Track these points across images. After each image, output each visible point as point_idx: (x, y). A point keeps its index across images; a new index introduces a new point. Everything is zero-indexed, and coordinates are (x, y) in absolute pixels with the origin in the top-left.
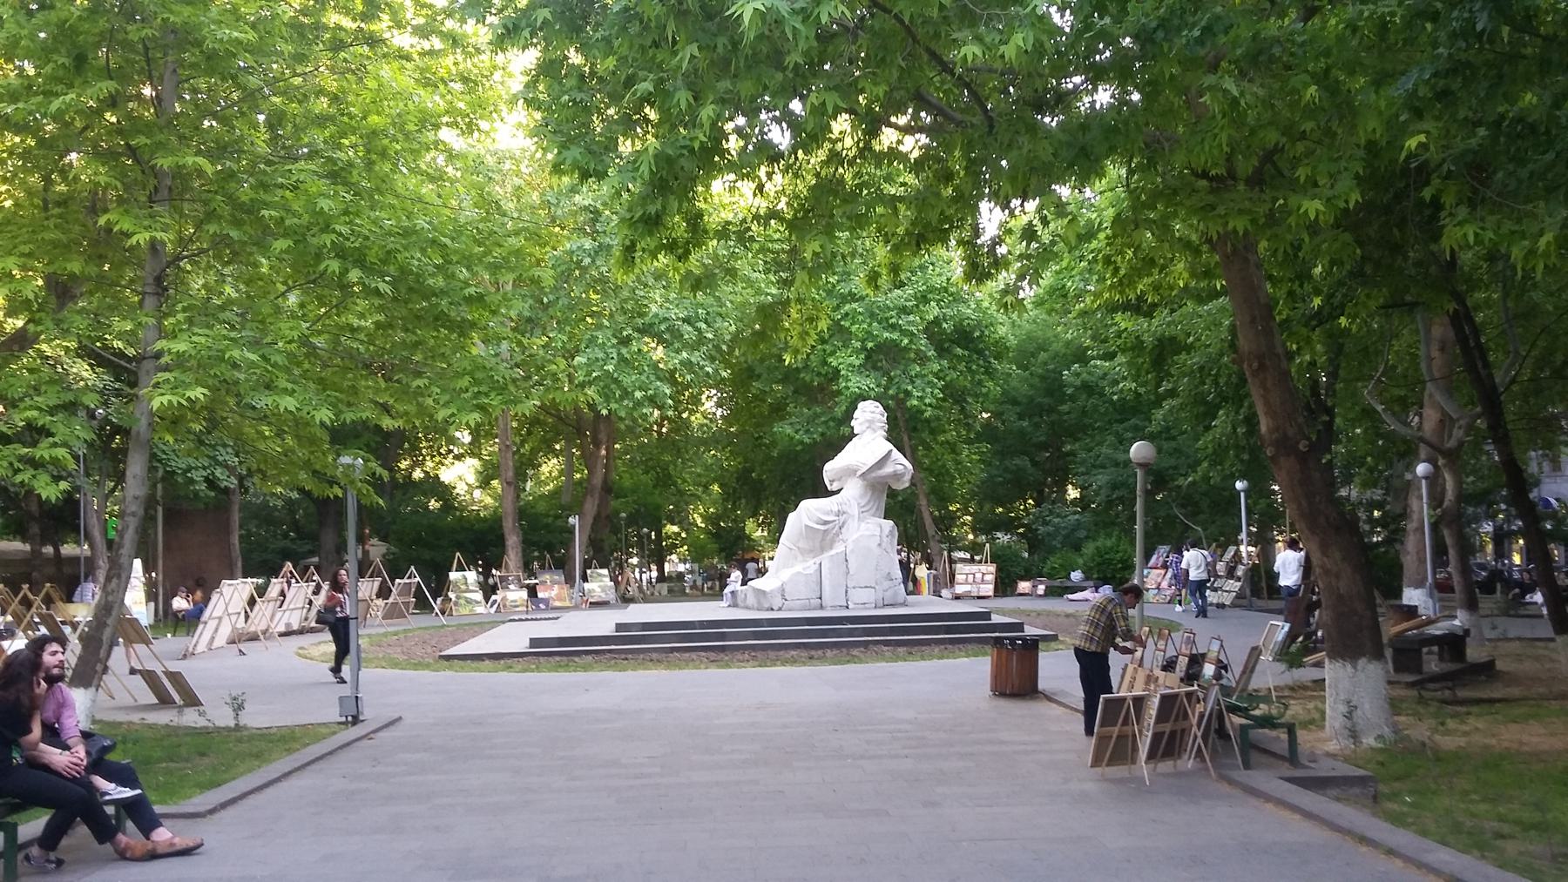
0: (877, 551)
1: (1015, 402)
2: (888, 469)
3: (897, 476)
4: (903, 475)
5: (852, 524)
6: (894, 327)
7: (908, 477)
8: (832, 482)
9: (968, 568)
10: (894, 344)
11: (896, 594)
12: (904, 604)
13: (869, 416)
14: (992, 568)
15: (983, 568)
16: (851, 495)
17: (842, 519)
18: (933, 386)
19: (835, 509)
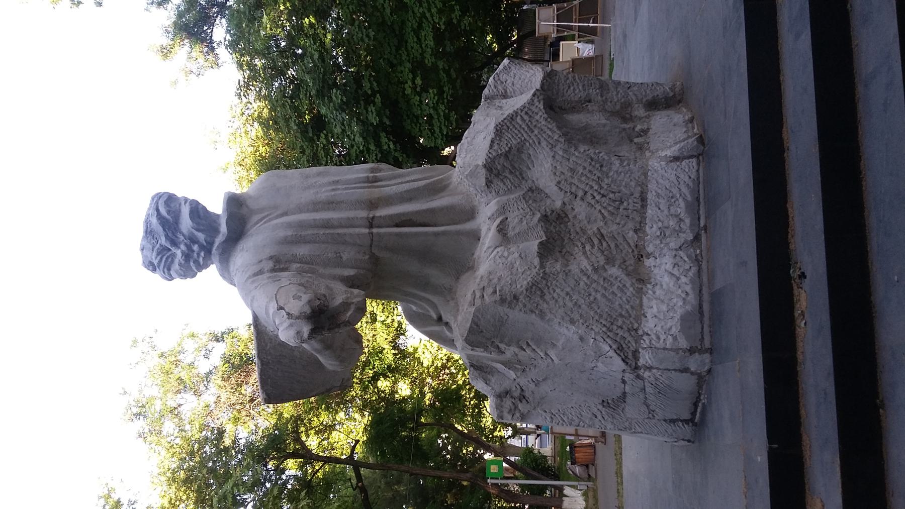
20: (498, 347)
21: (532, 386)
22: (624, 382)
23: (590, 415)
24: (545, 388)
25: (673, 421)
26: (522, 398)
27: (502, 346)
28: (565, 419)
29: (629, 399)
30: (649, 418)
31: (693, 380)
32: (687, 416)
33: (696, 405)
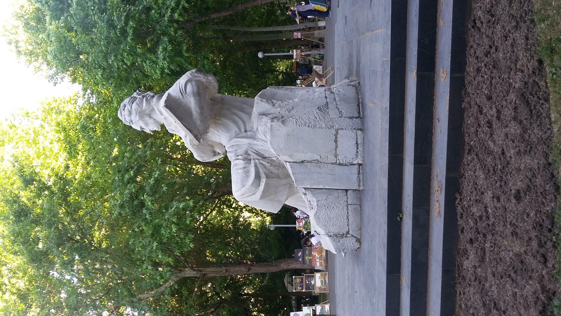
2: (192, 102)
3: (200, 93)
5: (259, 146)
7: (201, 77)
8: (215, 154)
10: (135, 30)
11: (344, 100)
12: (355, 75)
13: (135, 118)
16: (224, 140)
17: (253, 156)
19: (241, 163)
21: (287, 113)
22: (326, 97)
23: (313, 118)
24: (293, 112)
25: (351, 118)
26: (283, 117)
27: (274, 101)
28: (302, 122)
29: (330, 106)
30: (340, 117)
31: (354, 90)
32: (356, 115)
33: (358, 106)
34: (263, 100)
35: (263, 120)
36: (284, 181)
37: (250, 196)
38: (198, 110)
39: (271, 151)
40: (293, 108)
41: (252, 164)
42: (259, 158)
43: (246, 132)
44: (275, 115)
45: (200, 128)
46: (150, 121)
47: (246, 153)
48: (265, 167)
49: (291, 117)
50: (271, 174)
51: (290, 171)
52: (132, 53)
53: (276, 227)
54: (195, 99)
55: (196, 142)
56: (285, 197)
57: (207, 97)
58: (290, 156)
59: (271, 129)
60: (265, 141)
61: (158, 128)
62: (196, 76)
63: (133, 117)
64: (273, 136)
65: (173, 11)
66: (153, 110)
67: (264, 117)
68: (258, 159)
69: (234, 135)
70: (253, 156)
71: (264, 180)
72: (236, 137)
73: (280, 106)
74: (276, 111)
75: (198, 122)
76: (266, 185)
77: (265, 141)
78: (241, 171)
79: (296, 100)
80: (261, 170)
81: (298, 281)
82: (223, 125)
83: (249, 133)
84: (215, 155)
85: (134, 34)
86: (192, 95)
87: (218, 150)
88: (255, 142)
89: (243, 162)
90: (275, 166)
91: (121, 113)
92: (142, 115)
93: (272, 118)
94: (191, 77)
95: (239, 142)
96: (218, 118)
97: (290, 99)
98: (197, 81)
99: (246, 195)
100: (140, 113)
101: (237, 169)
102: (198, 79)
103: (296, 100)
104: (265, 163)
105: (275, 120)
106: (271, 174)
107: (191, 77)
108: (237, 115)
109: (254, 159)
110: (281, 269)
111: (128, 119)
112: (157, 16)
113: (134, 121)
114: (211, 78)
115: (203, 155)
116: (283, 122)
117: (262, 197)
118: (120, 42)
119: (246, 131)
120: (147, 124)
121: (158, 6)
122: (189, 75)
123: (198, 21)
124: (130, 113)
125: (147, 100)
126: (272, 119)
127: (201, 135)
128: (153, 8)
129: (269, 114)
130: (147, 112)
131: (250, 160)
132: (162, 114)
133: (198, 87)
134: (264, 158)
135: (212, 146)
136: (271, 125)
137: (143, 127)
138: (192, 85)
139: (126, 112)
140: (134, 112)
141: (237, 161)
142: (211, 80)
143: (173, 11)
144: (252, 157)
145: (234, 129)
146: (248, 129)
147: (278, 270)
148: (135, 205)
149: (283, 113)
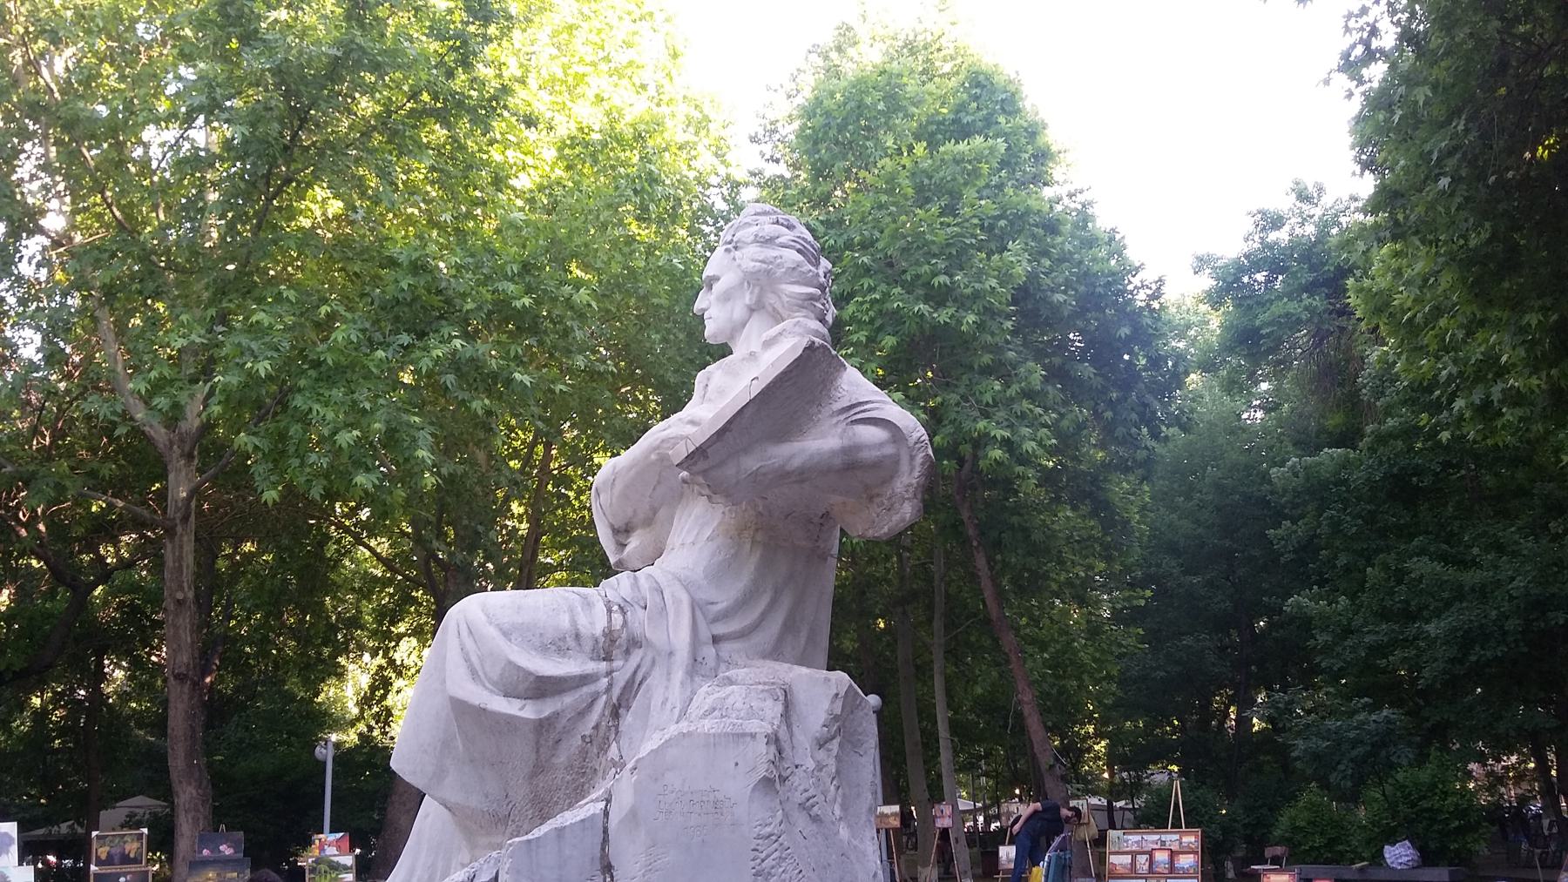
0: (754, 816)
1: (1172, 549)
2: (822, 441)
3: (857, 473)
4: (884, 469)
6: (939, 297)
7: (909, 477)
8: (622, 532)
9: (1133, 839)
13: (750, 257)
14: (1191, 839)
15: (1171, 838)
16: (683, 560)
17: (623, 669)
18: (1035, 423)
20: (833, 738)
21: (798, 798)
24: (801, 821)
26: (783, 780)
34: (839, 703)
35: (769, 702)
36: (520, 793)
37: (467, 660)
38: (796, 463)
39: (651, 733)
40: (816, 819)
41: (591, 667)
42: (616, 692)
43: (713, 645)
44: (787, 752)
45: (730, 471)
46: (739, 311)
47: (634, 643)
48: (582, 714)
49: (786, 815)
50: (550, 742)
51: (569, 818)
52: (878, 323)
53: (325, 763)
54: (833, 453)
55: (681, 452)
56: (455, 797)
57: (836, 499)
58: (633, 816)
59: (740, 736)
60: (684, 713)
61: (715, 336)
62: (912, 458)
63: (753, 251)
64: (714, 742)
65: (1007, 444)
66: (777, 318)
67: (779, 708)
68: (610, 685)
69: (702, 596)
70: (623, 669)
71: (526, 711)
72: (694, 605)
73: (820, 767)
74: (805, 755)
75: (751, 463)
76: (510, 720)
77: (684, 713)
78: (565, 622)
79: (844, 832)
80: (568, 699)
81: (128, 847)
82: (735, 556)
83: (709, 651)
84: (616, 531)
85: (936, 327)
86: (846, 442)
87: (634, 542)
88: (679, 675)
89: (598, 631)
90: (584, 754)
91: (765, 213)
92: (761, 280)
93: (777, 740)
94: (911, 442)
95: (678, 613)
96: (759, 537)
97: (844, 808)
98: (895, 459)
99: (469, 644)
100: (768, 272)
101: (571, 610)
102: (904, 466)
103: (844, 832)
104: (594, 716)
105: (773, 749)
106: (550, 742)
107: (911, 442)
108: (773, 603)
109: (609, 673)
110: (176, 787)
111: (747, 234)
112: (988, 398)
113: (738, 254)
114: (907, 511)
115: (619, 486)
116: (767, 783)
117: (461, 709)
118: (909, 288)
119: (716, 640)
120: (726, 297)
121: (1012, 399)
122: (916, 435)
123: (965, 515)
124: (769, 241)
125: (812, 298)
126: (774, 739)
127: (704, 473)
128: (1007, 386)
129: (789, 726)
130: (771, 299)
131: (608, 658)
132: (768, 344)
133: (876, 465)
134: (616, 712)
135: (648, 522)
136: (753, 736)
137: (717, 287)
138: (881, 445)
139: (769, 229)
140: (771, 253)
141: (601, 608)
142: (900, 509)
143: (1007, 444)
144: (617, 663)
145: (723, 598)
146: (727, 648)
147: (174, 776)
148: (419, 311)
149: (795, 780)
